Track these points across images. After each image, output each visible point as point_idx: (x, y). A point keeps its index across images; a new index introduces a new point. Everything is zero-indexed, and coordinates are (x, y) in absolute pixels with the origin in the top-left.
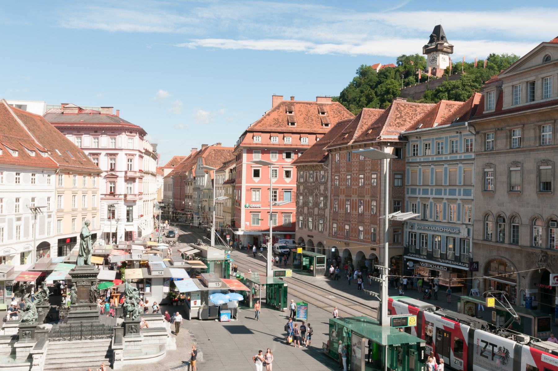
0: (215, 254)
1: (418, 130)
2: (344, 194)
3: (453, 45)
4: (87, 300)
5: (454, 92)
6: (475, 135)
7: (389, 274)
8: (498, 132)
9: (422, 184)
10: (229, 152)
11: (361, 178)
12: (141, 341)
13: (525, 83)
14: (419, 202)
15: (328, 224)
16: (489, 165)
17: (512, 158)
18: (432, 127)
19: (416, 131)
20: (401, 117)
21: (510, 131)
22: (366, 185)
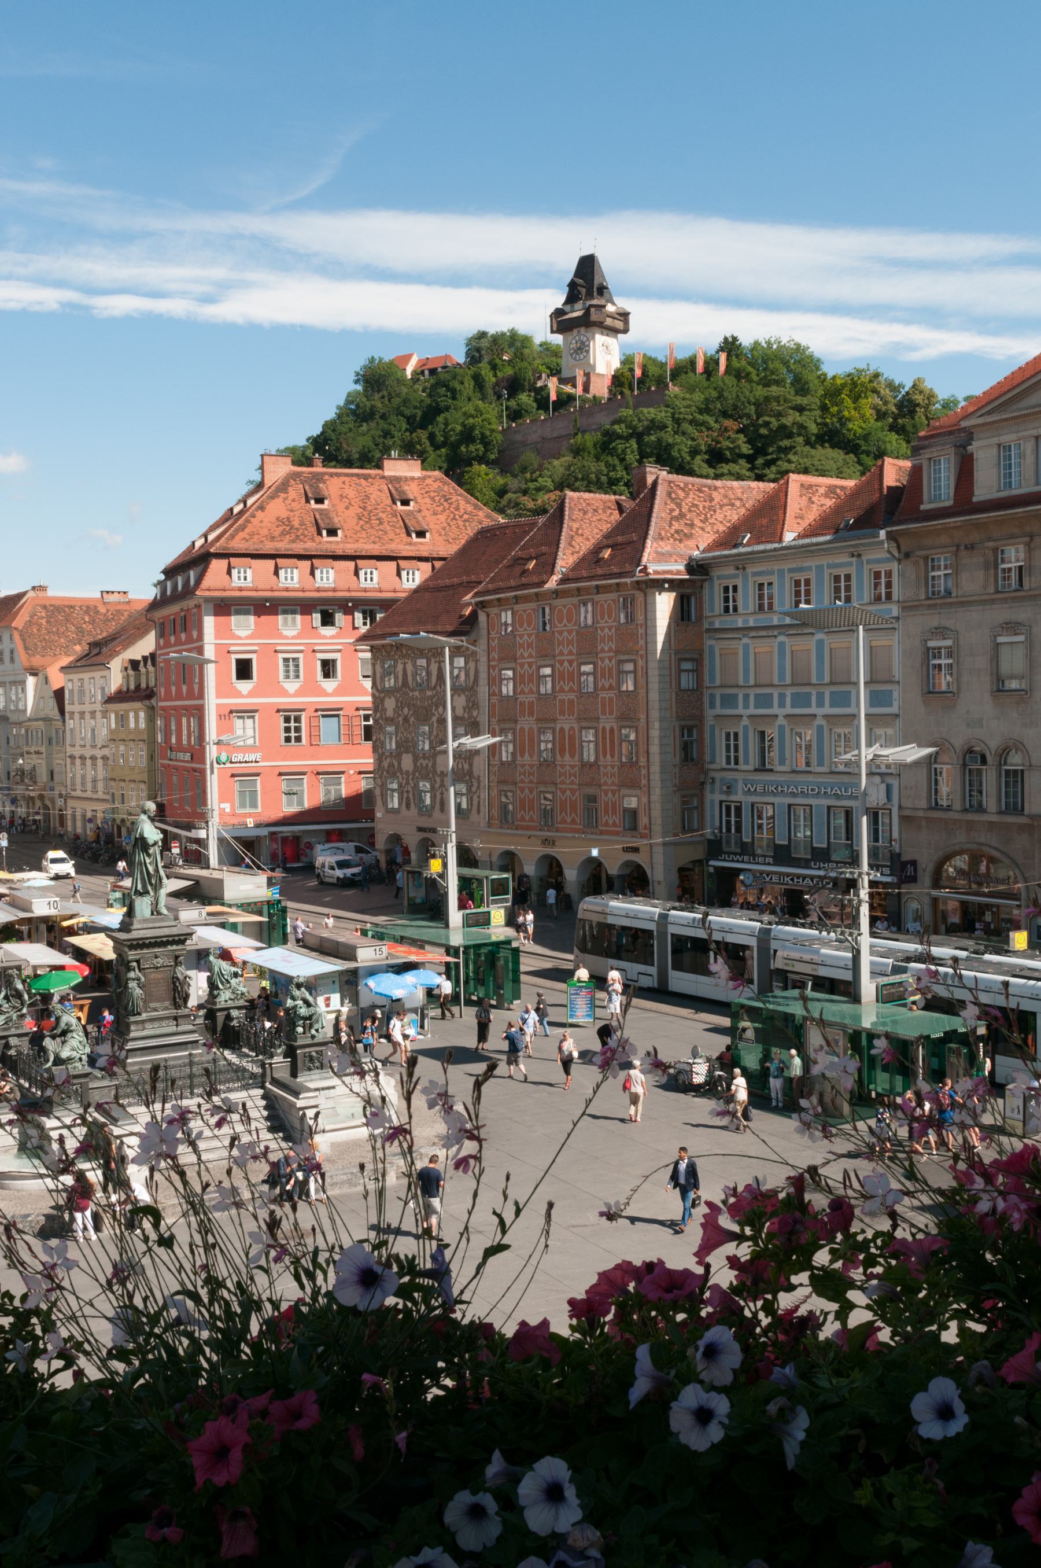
0: (242, 887)
1: (741, 550)
2: (611, 713)
3: (628, 310)
4: (167, 1003)
5: (653, 438)
6: (899, 561)
7: (870, 887)
8: (963, 553)
9: (752, 682)
10: (87, 612)
11: (588, 674)
12: (333, 1087)
13: (1033, 441)
14: (746, 728)
15: (484, 795)
16: (940, 632)
17: (1002, 614)
18: (781, 540)
19: (734, 551)
20: (682, 516)
21: (995, 550)
22: (603, 688)
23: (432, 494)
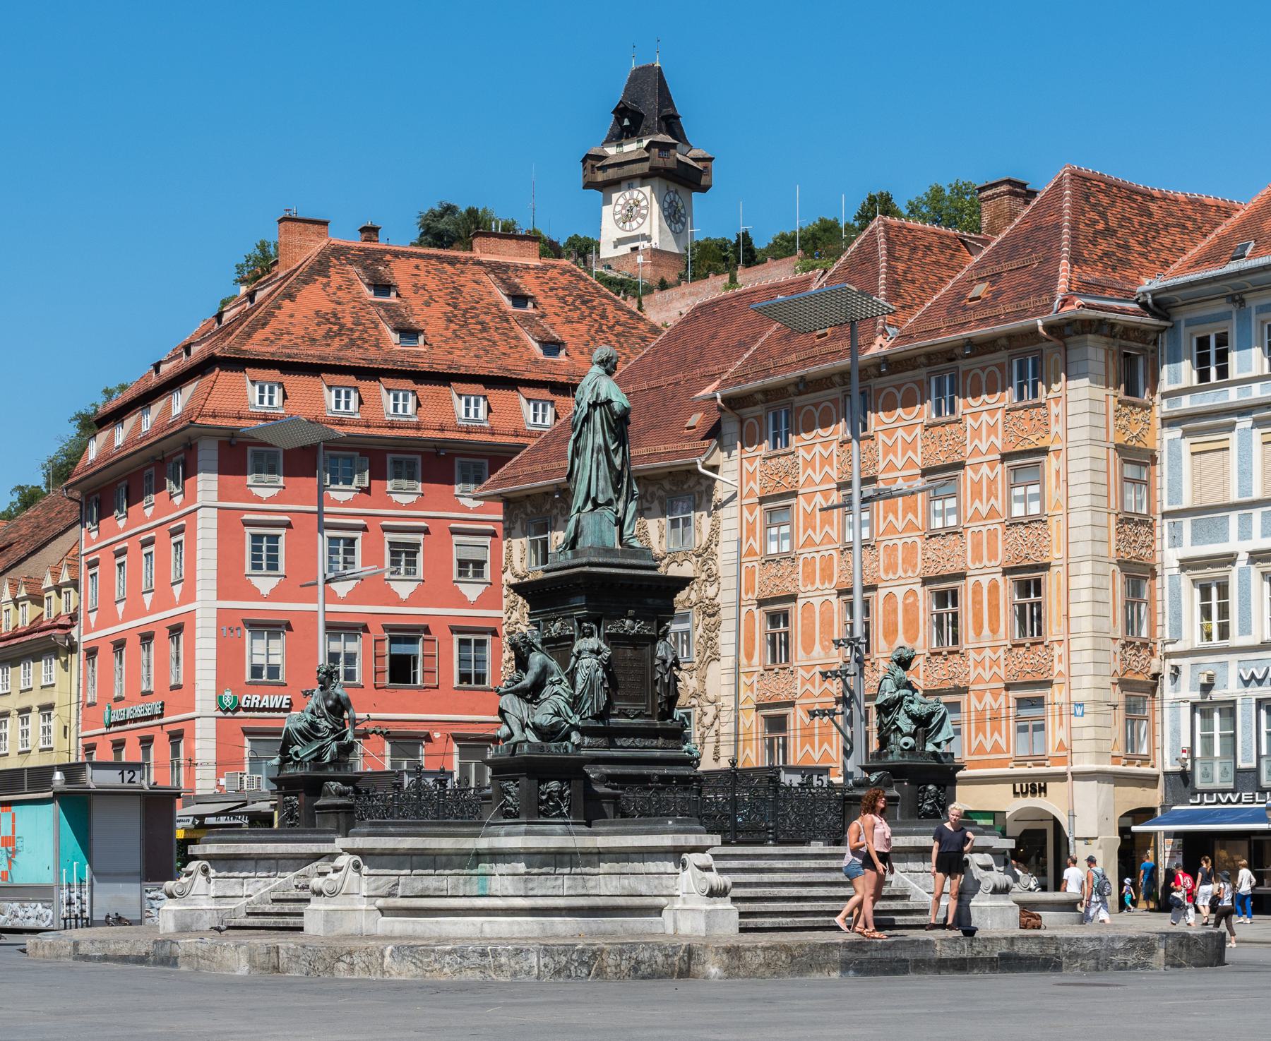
23: (561, 293)
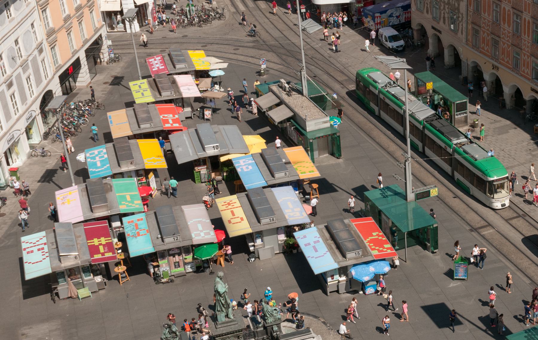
15: (464, 25)
